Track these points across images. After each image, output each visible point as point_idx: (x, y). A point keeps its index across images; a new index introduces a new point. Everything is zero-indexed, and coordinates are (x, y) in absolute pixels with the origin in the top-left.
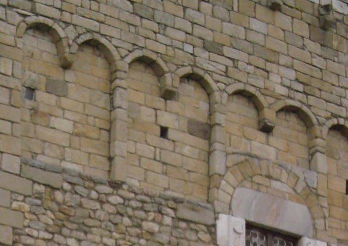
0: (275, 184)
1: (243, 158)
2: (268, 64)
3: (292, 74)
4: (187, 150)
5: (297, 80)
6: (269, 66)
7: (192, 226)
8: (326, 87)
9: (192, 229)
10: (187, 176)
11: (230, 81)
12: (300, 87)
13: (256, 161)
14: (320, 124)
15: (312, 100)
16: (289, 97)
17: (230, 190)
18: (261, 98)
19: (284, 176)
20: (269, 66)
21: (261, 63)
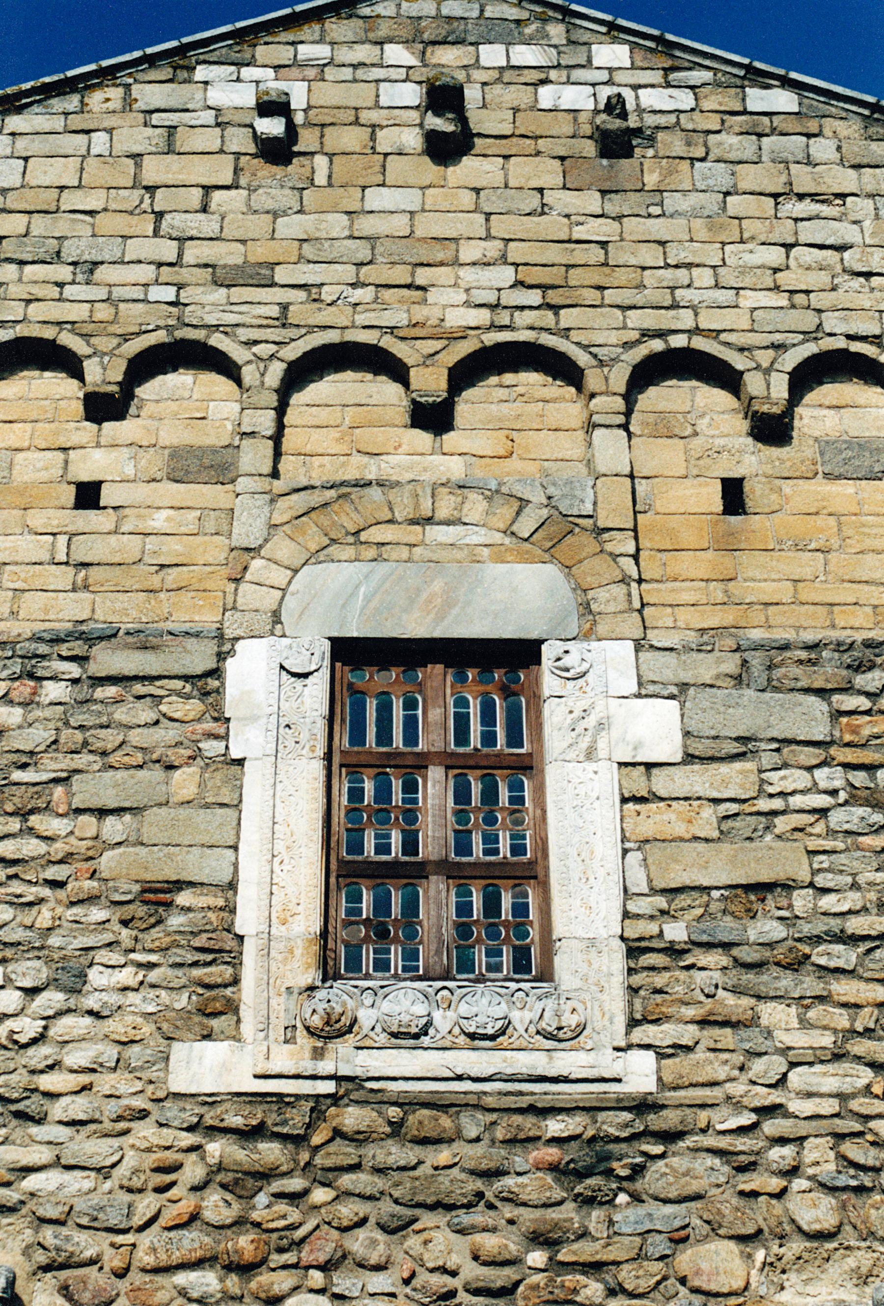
0: (438, 534)
1: (332, 493)
2: (420, 271)
3: (507, 275)
4: (159, 520)
5: (519, 284)
6: (423, 276)
7: (139, 688)
8: (622, 276)
9: (139, 697)
10: (155, 581)
11: (293, 333)
12: (534, 297)
13: (375, 493)
14: (601, 363)
15: (568, 318)
16: (493, 327)
17: (280, 576)
18: (400, 350)
19: (475, 507)
20: (423, 276)
21: (401, 275)
